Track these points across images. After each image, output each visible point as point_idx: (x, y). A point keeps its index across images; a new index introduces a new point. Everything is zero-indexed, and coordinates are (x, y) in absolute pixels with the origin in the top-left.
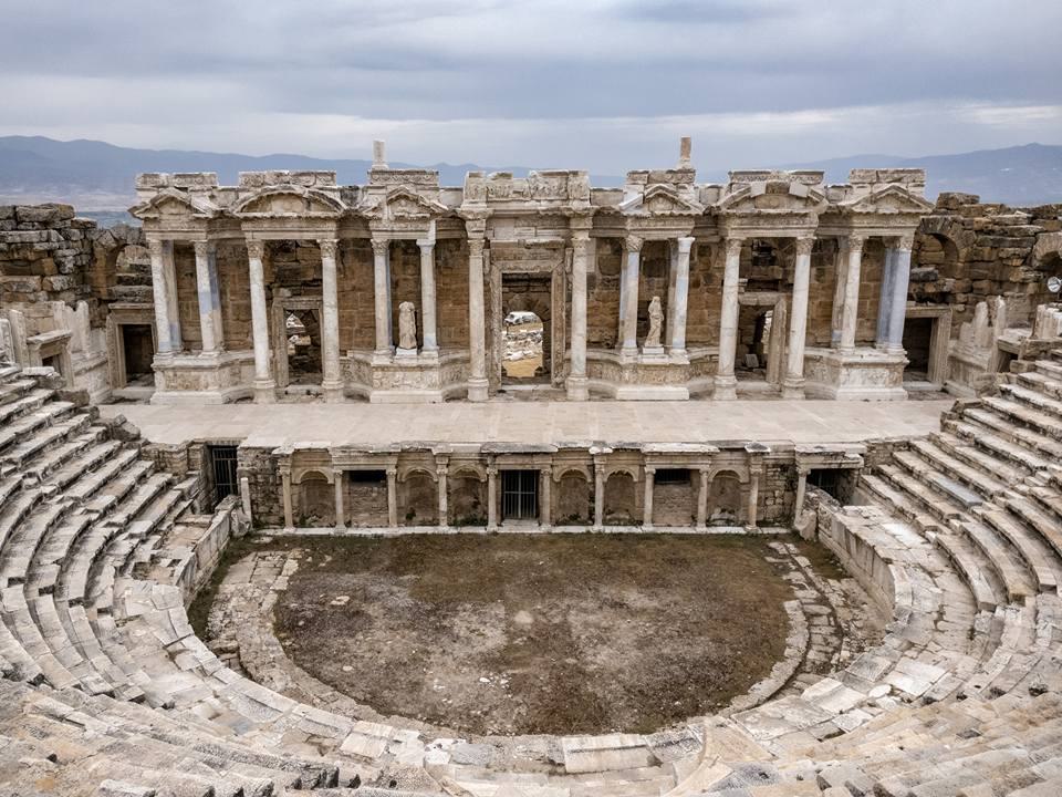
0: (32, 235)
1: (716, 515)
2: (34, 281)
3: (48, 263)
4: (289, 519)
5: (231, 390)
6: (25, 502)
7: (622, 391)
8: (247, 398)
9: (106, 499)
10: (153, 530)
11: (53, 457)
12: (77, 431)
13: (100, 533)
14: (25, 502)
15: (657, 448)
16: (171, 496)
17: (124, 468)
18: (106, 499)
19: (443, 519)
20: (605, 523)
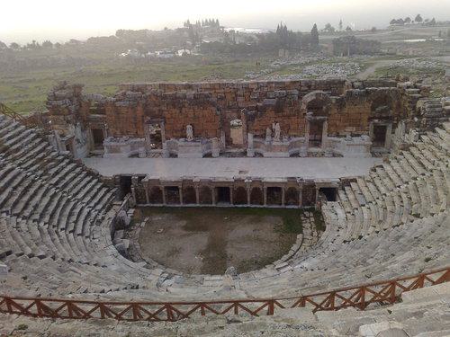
0: (60, 102)
1: (291, 200)
2: (61, 118)
3: (66, 111)
4: (148, 201)
5: (131, 152)
6: (63, 203)
7: (265, 154)
8: (137, 155)
9: (88, 198)
10: (103, 208)
11: (71, 186)
12: (78, 174)
13: (86, 210)
14: (63, 203)
15: (268, 180)
16: (109, 195)
17: (93, 186)
18: (88, 198)
19: (198, 201)
20: (252, 203)
